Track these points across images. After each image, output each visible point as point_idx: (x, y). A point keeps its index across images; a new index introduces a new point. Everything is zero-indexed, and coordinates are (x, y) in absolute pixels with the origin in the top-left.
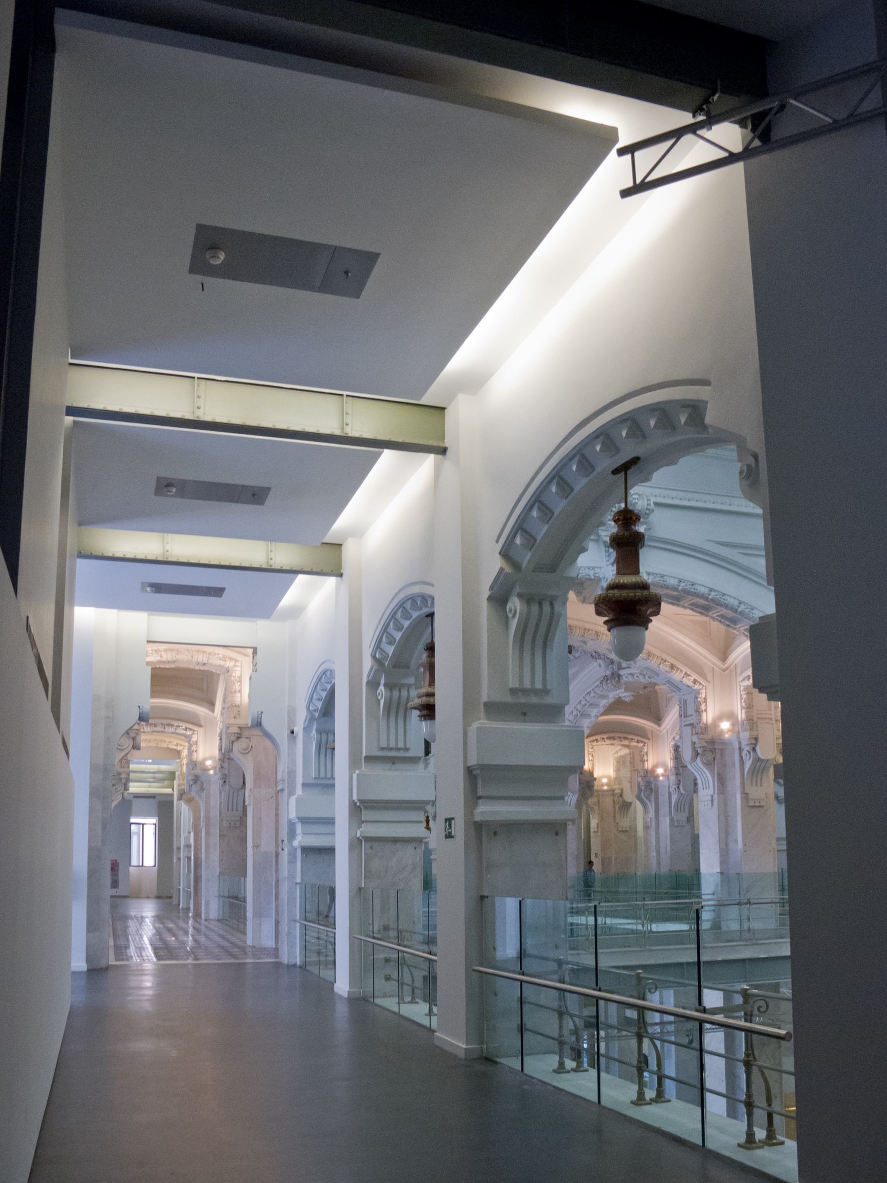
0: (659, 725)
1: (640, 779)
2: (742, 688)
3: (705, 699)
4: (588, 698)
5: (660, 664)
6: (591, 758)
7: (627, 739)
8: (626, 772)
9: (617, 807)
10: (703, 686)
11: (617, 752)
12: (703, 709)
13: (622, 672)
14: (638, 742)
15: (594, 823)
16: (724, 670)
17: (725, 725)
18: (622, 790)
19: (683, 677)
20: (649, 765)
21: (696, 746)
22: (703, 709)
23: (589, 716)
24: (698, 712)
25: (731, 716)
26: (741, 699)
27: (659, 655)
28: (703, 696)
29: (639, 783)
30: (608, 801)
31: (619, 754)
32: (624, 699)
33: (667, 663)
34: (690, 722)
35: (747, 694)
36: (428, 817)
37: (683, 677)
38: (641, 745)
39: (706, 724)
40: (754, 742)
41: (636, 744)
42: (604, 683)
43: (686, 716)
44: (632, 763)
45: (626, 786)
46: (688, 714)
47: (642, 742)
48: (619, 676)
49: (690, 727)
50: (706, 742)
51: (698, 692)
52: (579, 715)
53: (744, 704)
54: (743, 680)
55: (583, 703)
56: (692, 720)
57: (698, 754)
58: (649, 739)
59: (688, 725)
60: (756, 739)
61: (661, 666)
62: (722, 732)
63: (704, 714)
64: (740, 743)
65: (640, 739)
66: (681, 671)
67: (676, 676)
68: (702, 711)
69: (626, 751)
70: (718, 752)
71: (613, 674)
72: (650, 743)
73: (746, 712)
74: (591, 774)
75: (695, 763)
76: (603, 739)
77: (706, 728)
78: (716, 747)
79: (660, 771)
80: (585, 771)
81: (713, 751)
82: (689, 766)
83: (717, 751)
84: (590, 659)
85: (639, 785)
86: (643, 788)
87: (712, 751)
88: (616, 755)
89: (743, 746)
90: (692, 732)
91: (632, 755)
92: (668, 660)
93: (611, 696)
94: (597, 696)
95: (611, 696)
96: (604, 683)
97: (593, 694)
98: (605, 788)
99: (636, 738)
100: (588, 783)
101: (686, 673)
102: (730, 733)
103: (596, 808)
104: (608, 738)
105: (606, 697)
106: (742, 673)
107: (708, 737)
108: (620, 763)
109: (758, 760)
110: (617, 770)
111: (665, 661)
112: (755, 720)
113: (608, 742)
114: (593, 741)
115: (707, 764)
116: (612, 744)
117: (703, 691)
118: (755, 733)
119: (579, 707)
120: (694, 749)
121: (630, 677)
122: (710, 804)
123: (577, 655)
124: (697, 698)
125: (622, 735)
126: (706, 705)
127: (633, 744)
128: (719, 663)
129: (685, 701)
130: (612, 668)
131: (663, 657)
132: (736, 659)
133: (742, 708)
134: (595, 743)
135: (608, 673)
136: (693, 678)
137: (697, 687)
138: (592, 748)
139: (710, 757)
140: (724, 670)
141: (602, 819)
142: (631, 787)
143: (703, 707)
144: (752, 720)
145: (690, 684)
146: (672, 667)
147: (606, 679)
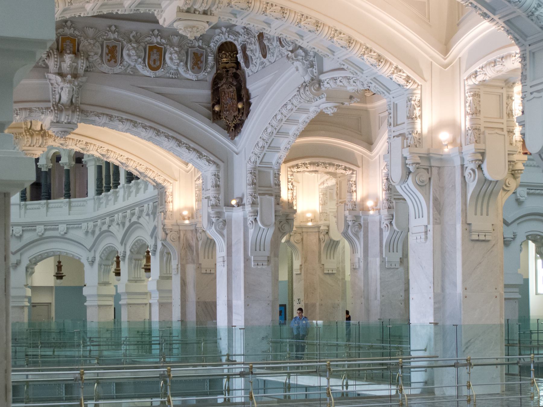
0: (370, 150)
1: (347, 213)
2: (467, 88)
3: (420, 101)
4: (284, 111)
5: (364, 54)
6: (290, 186)
7: (333, 165)
8: (332, 206)
9: (323, 245)
10: (418, 85)
11: (323, 183)
12: (418, 115)
13: (322, 77)
14: (345, 169)
15: (297, 264)
16: (445, 66)
17: (444, 136)
18: (328, 227)
19: (393, 73)
20: (358, 196)
21: (407, 162)
22: (418, 115)
23: (286, 134)
24: (411, 118)
25: (452, 125)
26: (466, 102)
27: (363, 42)
28: (418, 98)
29: (346, 217)
30: (313, 239)
31: (326, 185)
32: (326, 111)
33: (372, 53)
34: (401, 132)
35: (473, 95)
36: (118, 258)
37: (393, 73)
38: (349, 172)
39: (421, 134)
40: (481, 158)
41: (344, 172)
42: (302, 91)
43: (396, 125)
44: (339, 194)
45: (332, 221)
46: (398, 123)
47: (350, 169)
48: (320, 82)
49: (400, 138)
50: (420, 157)
51: (412, 93)
52: (275, 132)
53: (468, 109)
54: (469, 77)
55: (279, 117)
56: (404, 129)
57: (410, 173)
58: (359, 167)
59: (398, 136)
60: (483, 154)
61: (365, 57)
62: (441, 145)
63: (418, 121)
64: (462, 159)
65: (348, 165)
66: (391, 64)
67: (385, 71)
68: (416, 117)
69: (332, 182)
70: (435, 171)
71: (312, 79)
72: (359, 170)
73: (471, 119)
74: (290, 205)
75: (406, 185)
76: (305, 164)
77: (420, 140)
78: (432, 164)
79: (370, 203)
80: (283, 202)
81: (428, 169)
82: (398, 188)
83: (433, 169)
84: (286, 60)
85: (346, 221)
86: (350, 223)
87: (428, 169)
88: (322, 187)
89: (466, 164)
90: (403, 143)
91: (339, 185)
92: (374, 49)
93: (312, 109)
94: (295, 109)
95: (312, 109)
96: (302, 91)
97: (289, 107)
98: (310, 224)
99: (344, 164)
100: (287, 215)
101: (396, 68)
102: (450, 147)
103: (299, 246)
104: (310, 164)
105: (306, 110)
106: (467, 69)
107: (423, 150)
108: (326, 195)
109: (485, 181)
110: (324, 204)
111: (371, 51)
112: (482, 129)
113: (311, 168)
114: (293, 167)
115: (420, 186)
116: (316, 171)
117: (419, 92)
118: (481, 146)
119: (274, 123)
120: (405, 165)
121: (332, 83)
122: (423, 237)
123: (272, 59)
124: (410, 100)
125: (327, 161)
126: (421, 110)
127: (340, 171)
128: (438, 56)
129: (396, 106)
130: (312, 71)
131: (368, 46)
132: (460, 51)
133: (466, 113)
134: (295, 170)
135: (307, 78)
136: (405, 75)
137: (409, 86)
138: (292, 175)
139: (425, 176)
140: (445, 66)
141: (305, 260)
142: (337, 223)
143: (417, 112)
144: (479, 129)
145: (402, 82)
146: (379, 58)
147: (305, 86)
